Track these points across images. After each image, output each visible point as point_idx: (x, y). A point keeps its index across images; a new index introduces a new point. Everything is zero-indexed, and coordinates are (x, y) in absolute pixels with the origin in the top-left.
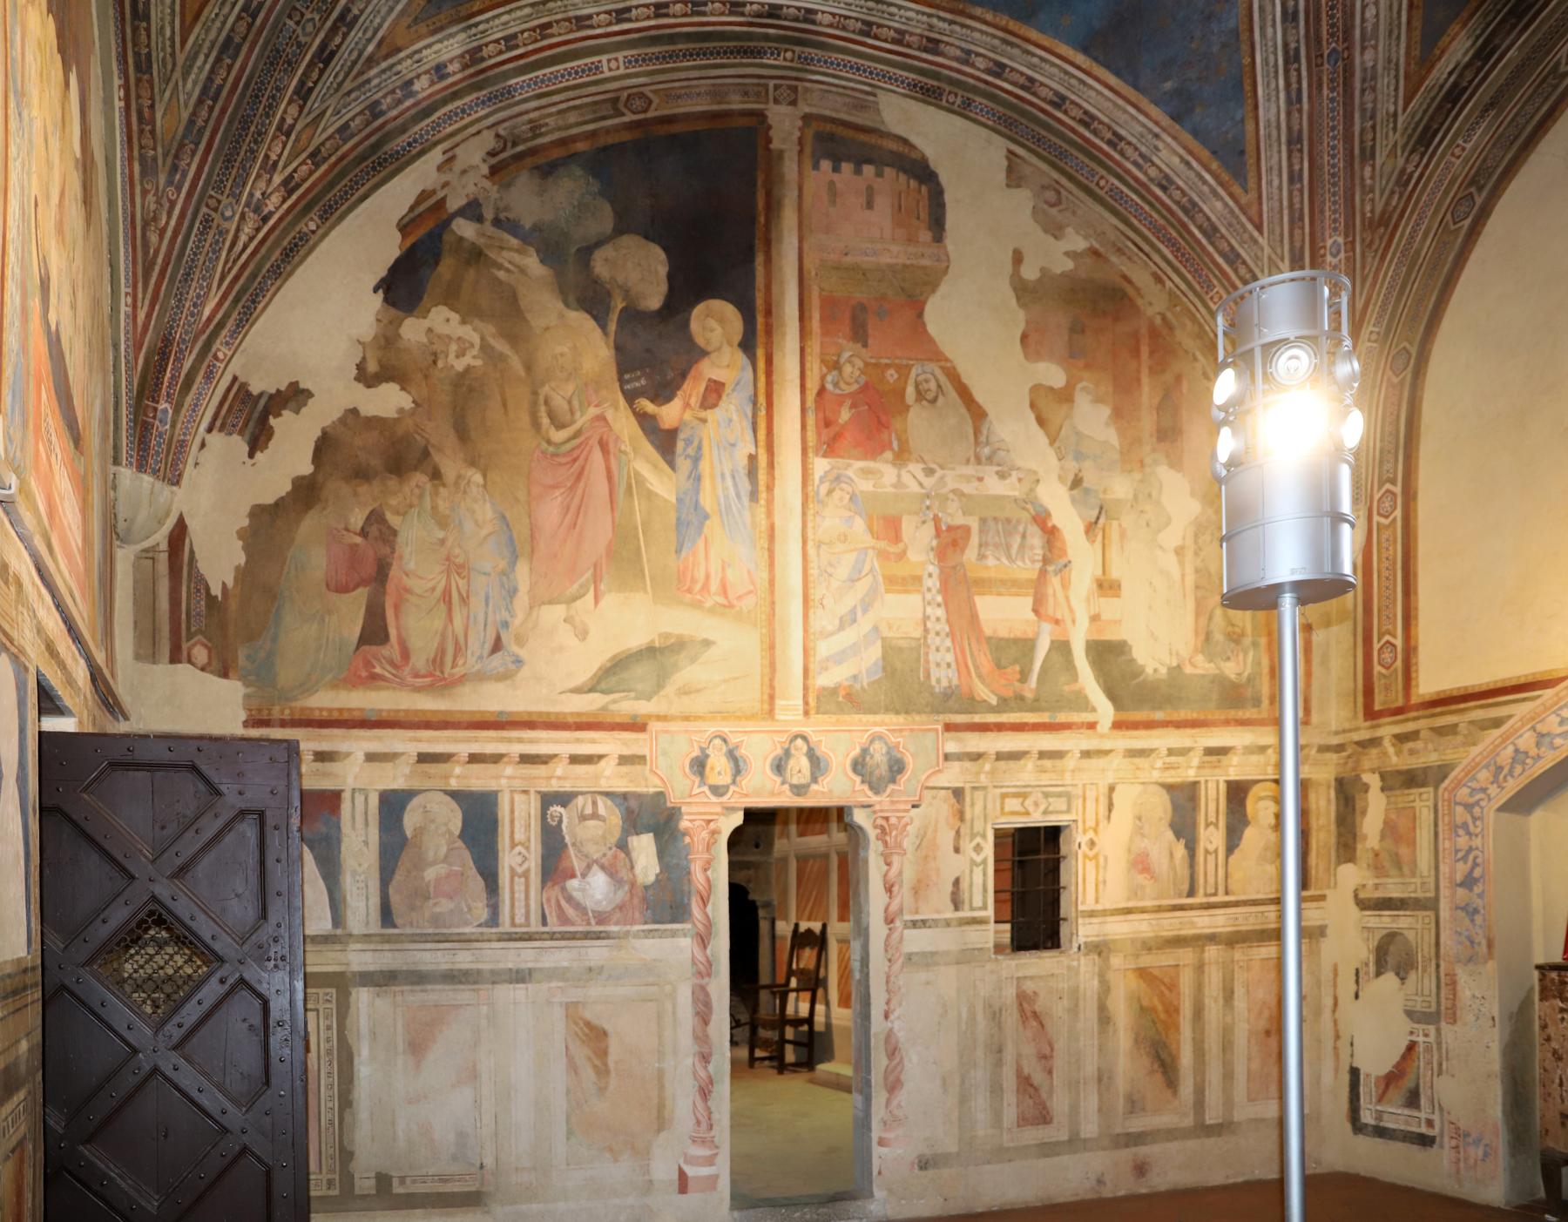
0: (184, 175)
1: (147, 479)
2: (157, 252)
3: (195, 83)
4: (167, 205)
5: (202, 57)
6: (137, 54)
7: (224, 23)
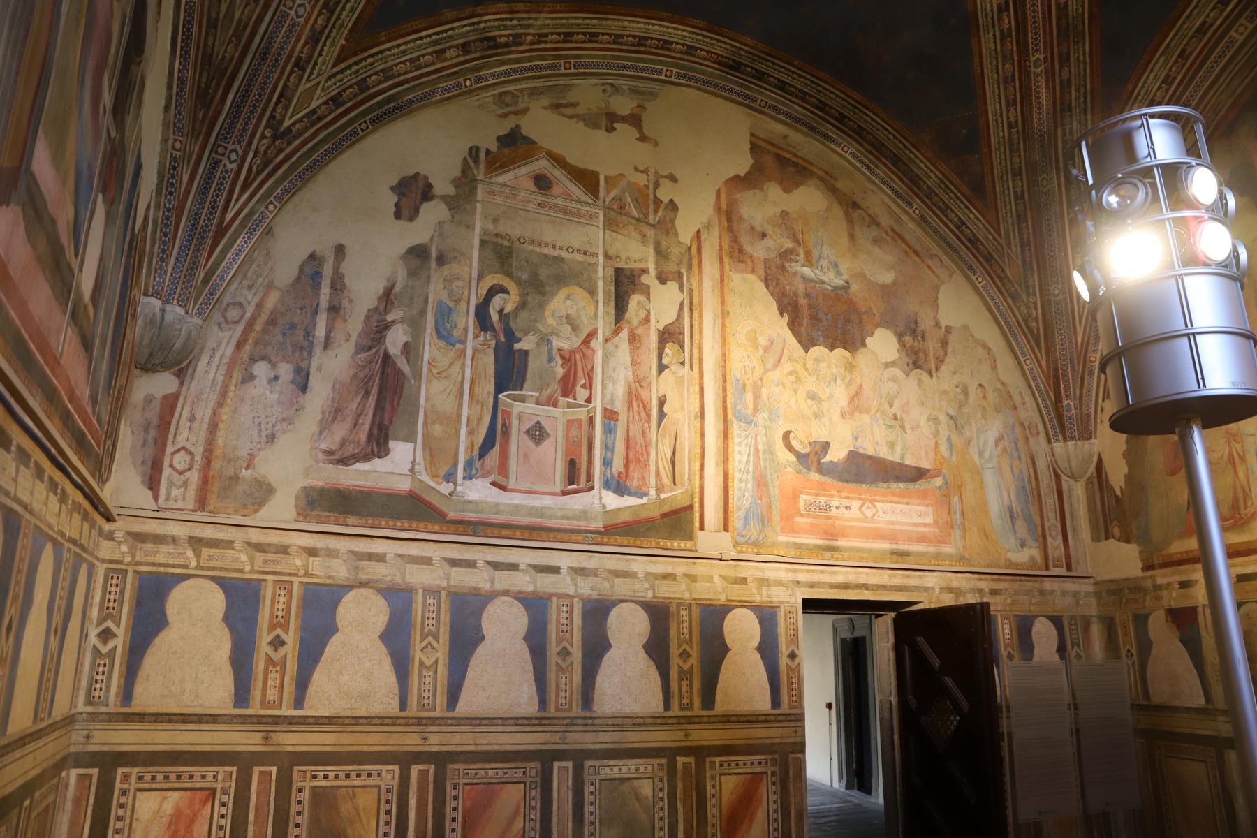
0: (1034, 286)
1: (1071, 444)
2: (1038, 329)
3: (1016, 246)
4: (1032, 306)
5: (1012, 234)
6: (984, 257)
7: (1011, 213)
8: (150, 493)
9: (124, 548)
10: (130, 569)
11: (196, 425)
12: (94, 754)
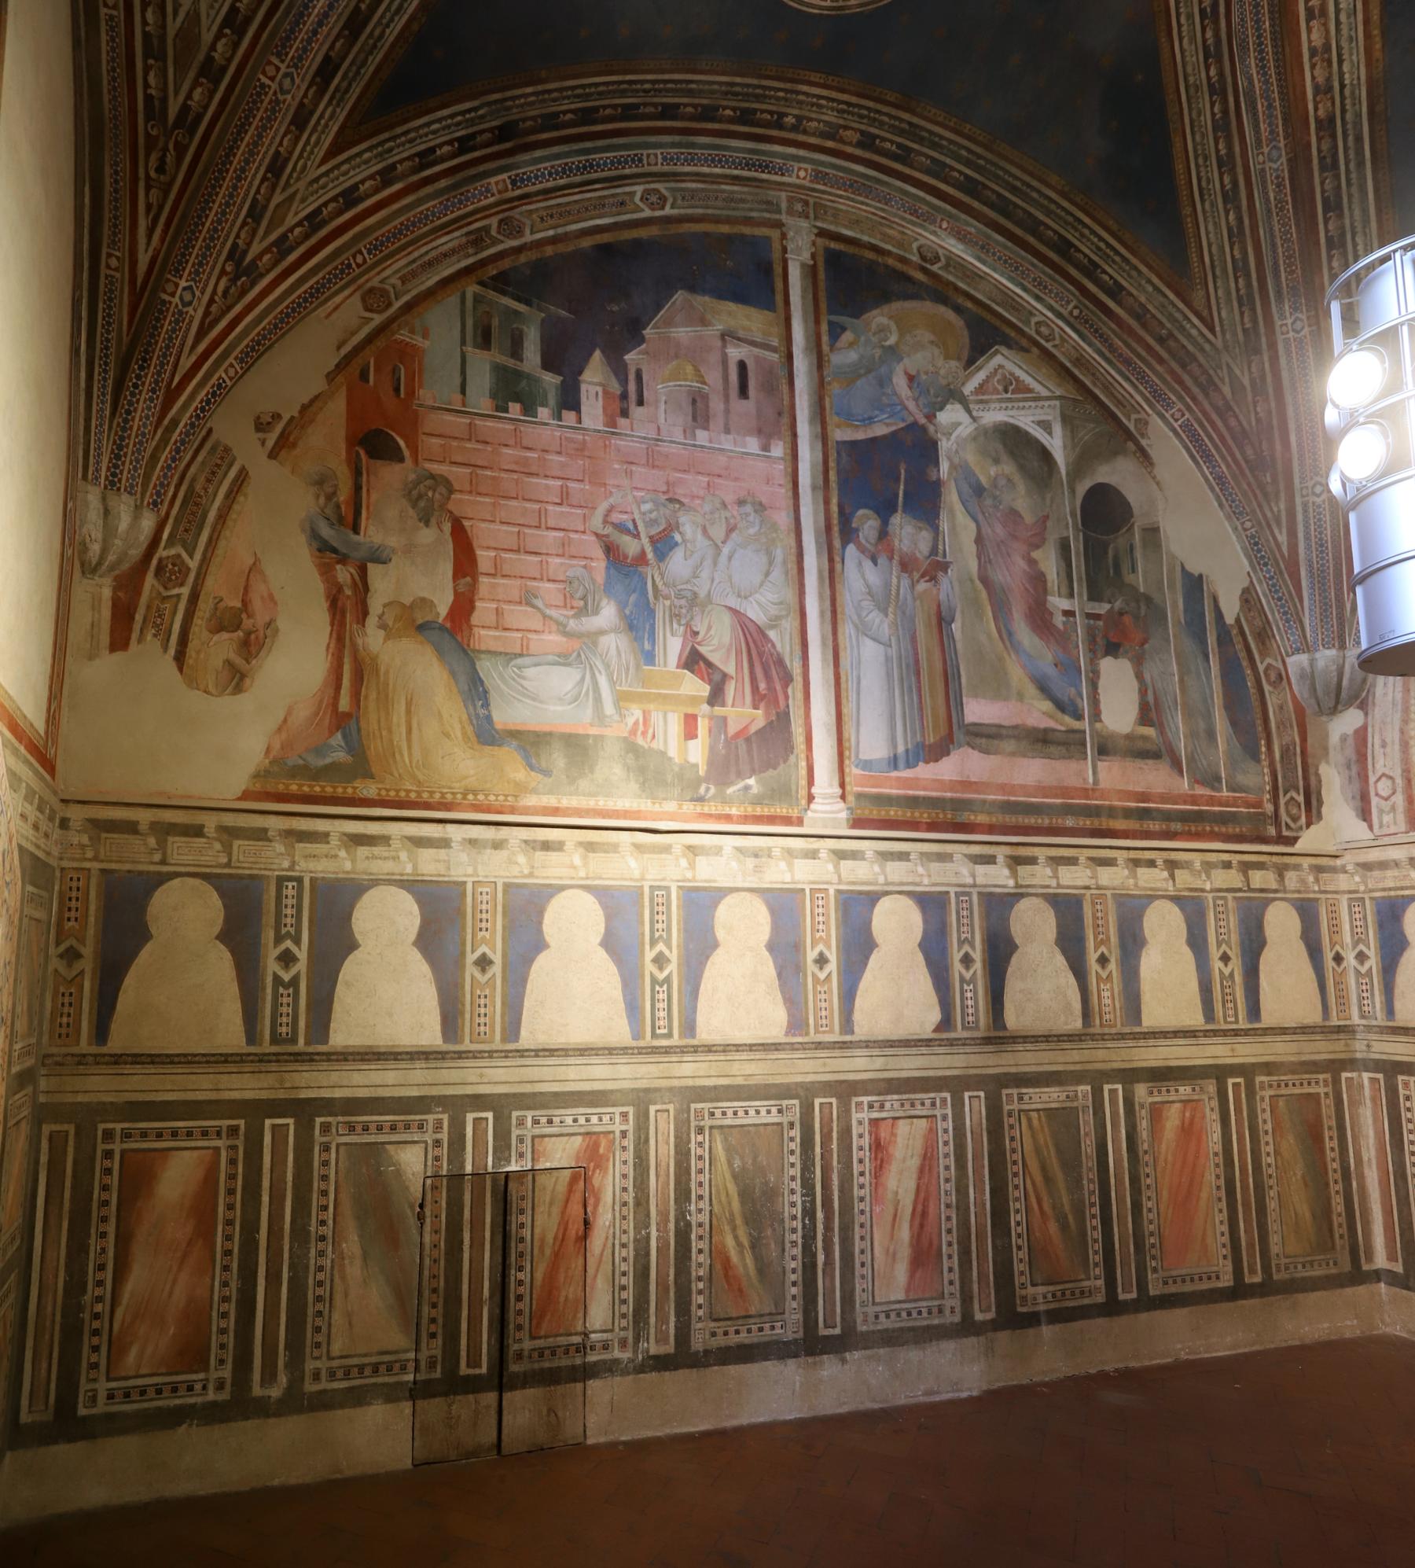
8: (1365, 825)
9: (1357, 879)
10: (1366, 896)
11: (1388, 750)
12: (1377, 1062)
